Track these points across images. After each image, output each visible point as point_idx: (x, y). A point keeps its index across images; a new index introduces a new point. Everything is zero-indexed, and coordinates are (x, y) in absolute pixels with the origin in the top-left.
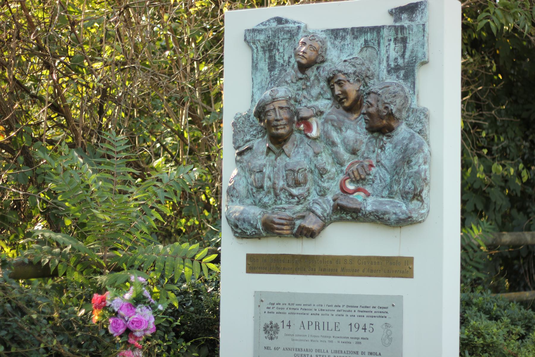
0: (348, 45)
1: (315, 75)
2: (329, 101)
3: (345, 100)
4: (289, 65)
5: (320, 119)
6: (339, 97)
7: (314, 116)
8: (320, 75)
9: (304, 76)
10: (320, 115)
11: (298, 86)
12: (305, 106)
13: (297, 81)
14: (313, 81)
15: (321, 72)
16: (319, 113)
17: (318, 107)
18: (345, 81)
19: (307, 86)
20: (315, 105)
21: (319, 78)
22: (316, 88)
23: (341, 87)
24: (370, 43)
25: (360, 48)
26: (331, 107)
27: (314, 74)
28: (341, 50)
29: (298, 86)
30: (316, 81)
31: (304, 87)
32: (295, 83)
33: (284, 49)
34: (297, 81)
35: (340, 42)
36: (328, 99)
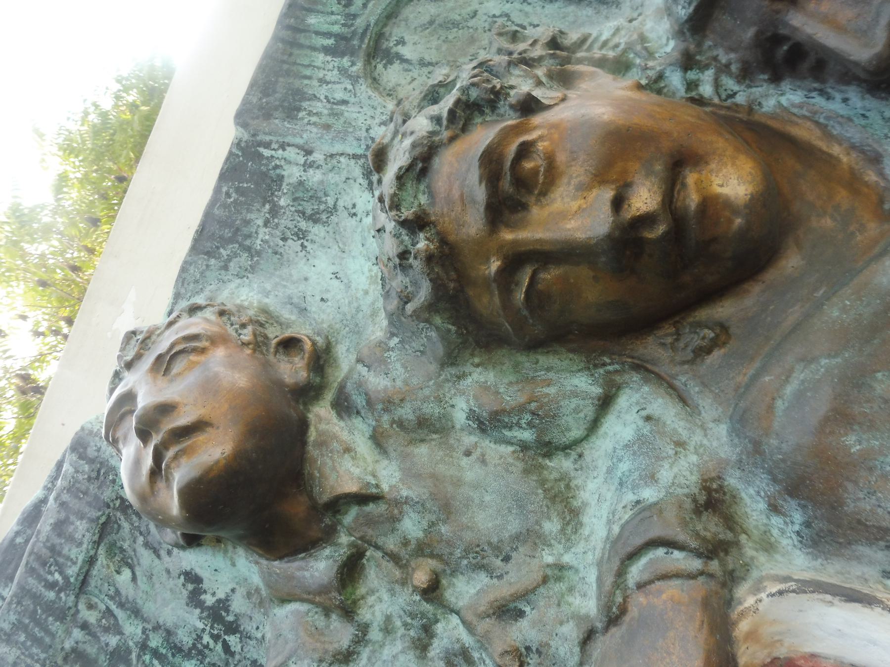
0: (307, 166)
1: (378, 440)
2: (624, 400)
3: (691, 178)
4: (233, 628)
5: (768, 546)
6: (646, 220)
7: (731, 579)
8: (389, 404)
9: (344, 539)
10: (730, 522)
11: (387, 629)
12: (588, 638)
13: (348, 612)
14: (410, 474)
15: (377, 382)
16: (711, 526)
17: (643, 510)
18: (516, 130)
19: (422, 549)
20: (614, 542)
21: (406, 412)
22: (470, 471)
23: (552, 173)
24: (360, 23)
25: (364, 89)
26: (683, 399)
27: (363, 446)
28: (314, 219)
29: (387, 629)
30: (422, 451)
31: (421, 578)
32: (362, 637)
33: (136, 612)
34: (348, 612)
35: (275, 211)
36: (605, 403)
